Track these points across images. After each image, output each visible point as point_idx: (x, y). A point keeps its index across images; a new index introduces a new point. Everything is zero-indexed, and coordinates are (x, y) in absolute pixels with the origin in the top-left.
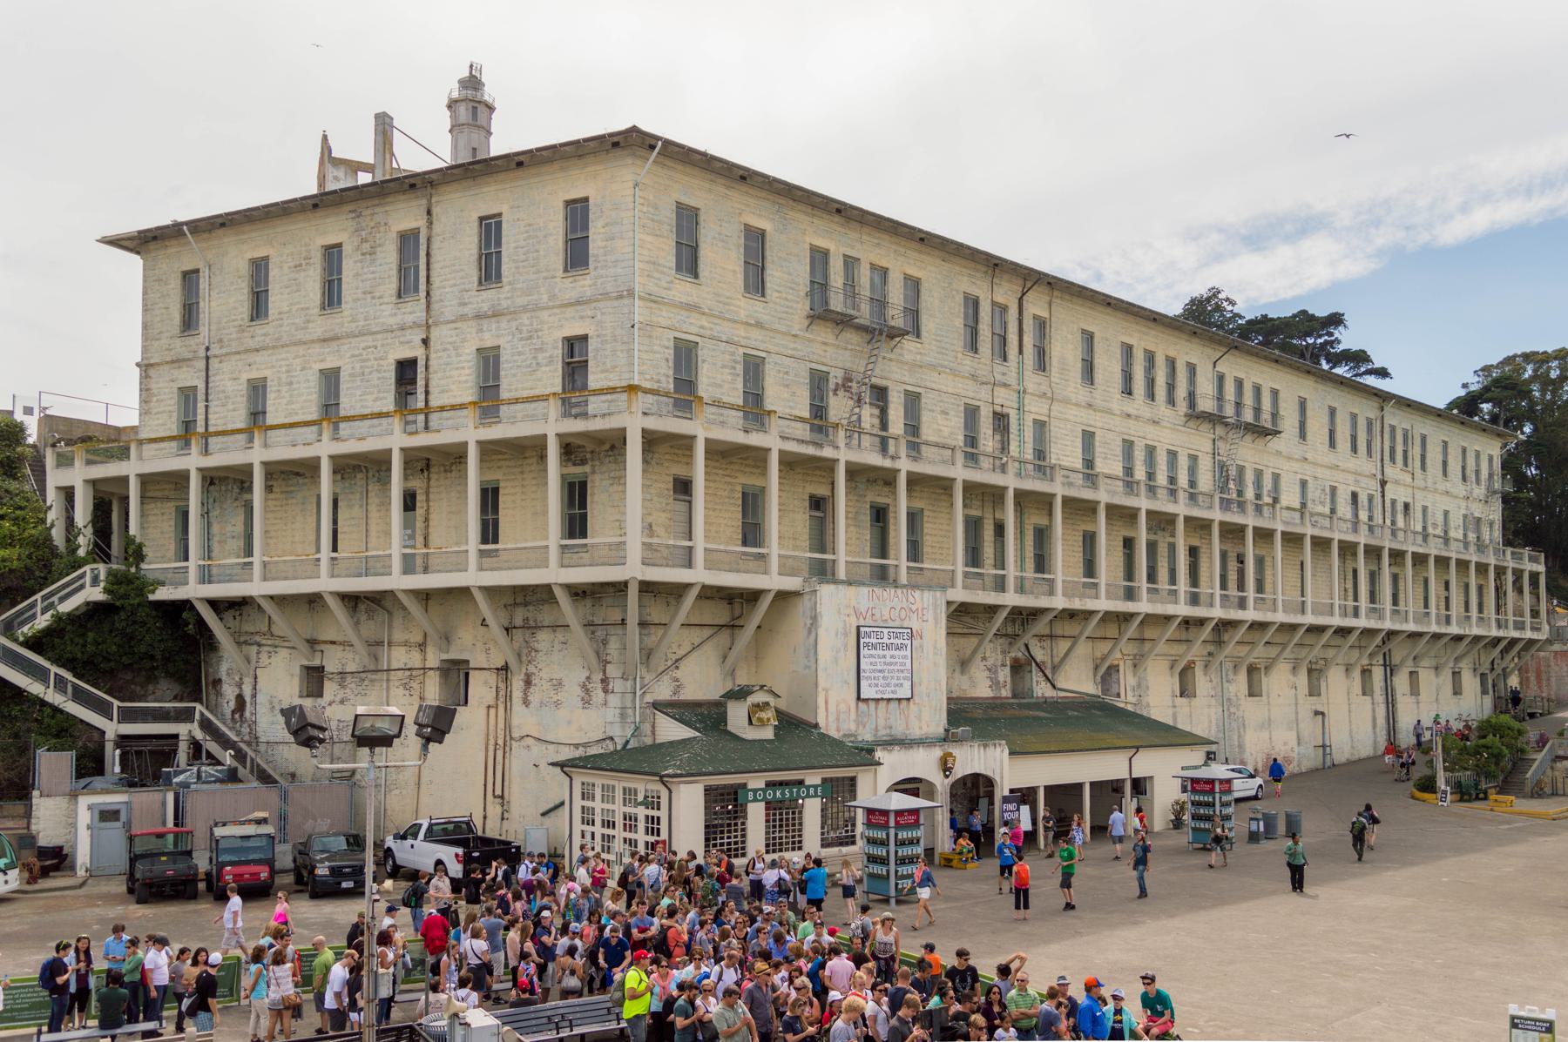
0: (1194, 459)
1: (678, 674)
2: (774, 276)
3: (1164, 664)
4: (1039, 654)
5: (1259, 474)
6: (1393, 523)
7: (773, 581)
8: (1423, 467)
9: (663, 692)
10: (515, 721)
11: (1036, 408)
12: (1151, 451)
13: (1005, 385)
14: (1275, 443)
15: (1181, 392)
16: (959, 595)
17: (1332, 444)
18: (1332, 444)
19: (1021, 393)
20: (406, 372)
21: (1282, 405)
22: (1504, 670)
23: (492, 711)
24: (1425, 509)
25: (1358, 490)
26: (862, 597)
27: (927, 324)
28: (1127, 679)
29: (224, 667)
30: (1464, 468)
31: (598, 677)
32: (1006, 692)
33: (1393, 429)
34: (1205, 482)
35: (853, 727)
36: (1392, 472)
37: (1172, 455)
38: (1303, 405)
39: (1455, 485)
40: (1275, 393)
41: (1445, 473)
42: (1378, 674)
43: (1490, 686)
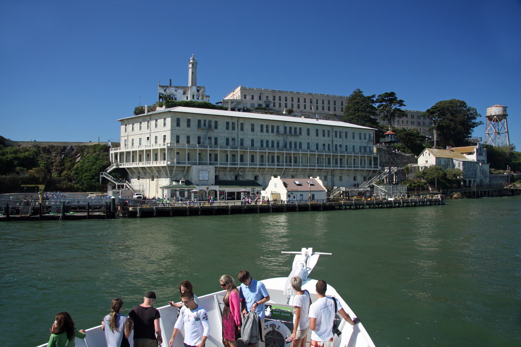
2: (192, 124)
4: (240, 173)
6: (336, 149)
7: (187, 165)
12: (267, 142)
16: (219, 166)
17: (317, 135)
18: (317, 135)
19: (238, 135)
20: (148, 138)
24: (346, 146)
26: (200, 167)
27: (219, 127)
34: (281, 145)
35: (198, 183)
36: (335, 139)
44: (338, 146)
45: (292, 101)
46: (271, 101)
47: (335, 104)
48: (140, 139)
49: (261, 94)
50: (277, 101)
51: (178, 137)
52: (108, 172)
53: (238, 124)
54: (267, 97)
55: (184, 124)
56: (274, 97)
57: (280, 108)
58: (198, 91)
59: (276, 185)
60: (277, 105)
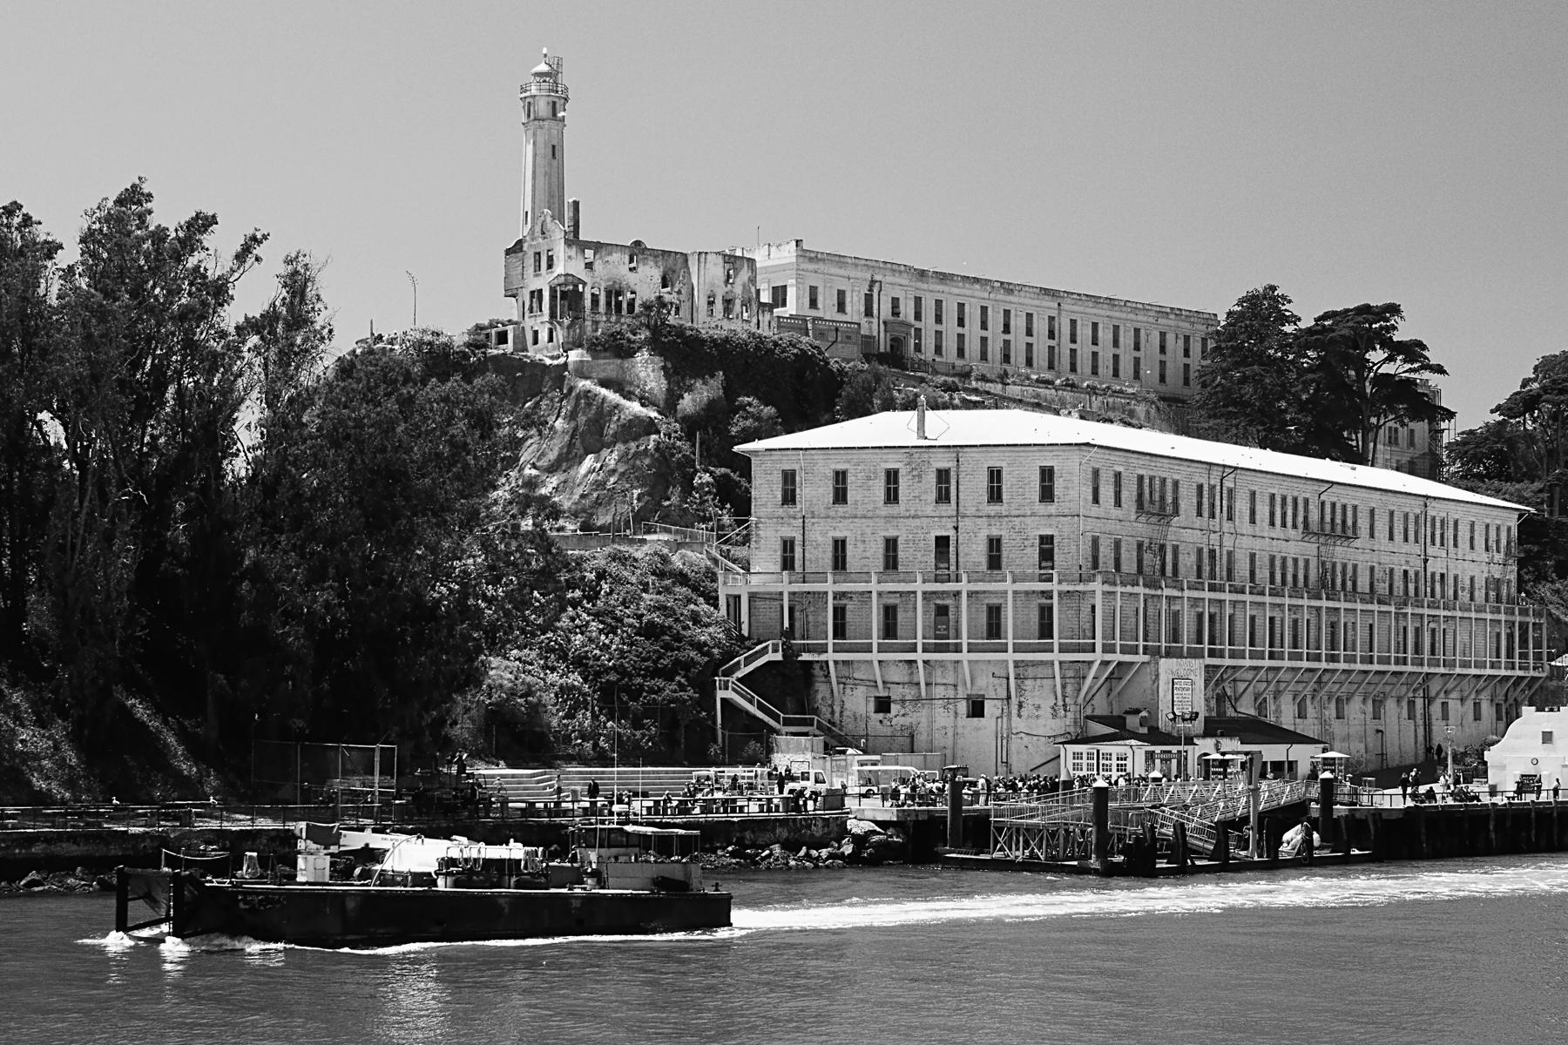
0: (1307, 562)
1: (1093, 702)
3: (1291, 697)
5: (1344, 566)
8: (1456, 545)
9: (1089, 712)
10: (1013, 725)
11: (1228, 543)
12: (1284, 560)
13: (1215, 532)
14: (1357, 543)
15: (1300, 519)
17: (1391, 538)
18: (1391, 538)
20: (942, 543)
21: (1359, 515)
22: (1515, 700)
23: (999, 720)
24: (1456, 578)
25: (1408, 568)
27: (1183, 505)
28: (1271, 706)
29: (819, 696)
30: (1487, 540)
31: (1060, 703)
32: (1214, 714)
33: (1434, 519)
36: (1430, 550)
37: (1295, 561)
39: (1480, 554)
40: (1355, 508)
41: (1472, 547)
43: (1504, 714)
44: (1438, 577)
45: (984, 326)
47: (1137, 347)
48: (891, 545)
49: (873, 282)
50: (928, 324)
51: (1095, 542)
52: (739, 674)
53: (1221, 493)
54: (895, 302)
55: (1107, 492)
56: (918, 300)
57: (937, 359)
59: (1547, 737)
60: (929, 343)
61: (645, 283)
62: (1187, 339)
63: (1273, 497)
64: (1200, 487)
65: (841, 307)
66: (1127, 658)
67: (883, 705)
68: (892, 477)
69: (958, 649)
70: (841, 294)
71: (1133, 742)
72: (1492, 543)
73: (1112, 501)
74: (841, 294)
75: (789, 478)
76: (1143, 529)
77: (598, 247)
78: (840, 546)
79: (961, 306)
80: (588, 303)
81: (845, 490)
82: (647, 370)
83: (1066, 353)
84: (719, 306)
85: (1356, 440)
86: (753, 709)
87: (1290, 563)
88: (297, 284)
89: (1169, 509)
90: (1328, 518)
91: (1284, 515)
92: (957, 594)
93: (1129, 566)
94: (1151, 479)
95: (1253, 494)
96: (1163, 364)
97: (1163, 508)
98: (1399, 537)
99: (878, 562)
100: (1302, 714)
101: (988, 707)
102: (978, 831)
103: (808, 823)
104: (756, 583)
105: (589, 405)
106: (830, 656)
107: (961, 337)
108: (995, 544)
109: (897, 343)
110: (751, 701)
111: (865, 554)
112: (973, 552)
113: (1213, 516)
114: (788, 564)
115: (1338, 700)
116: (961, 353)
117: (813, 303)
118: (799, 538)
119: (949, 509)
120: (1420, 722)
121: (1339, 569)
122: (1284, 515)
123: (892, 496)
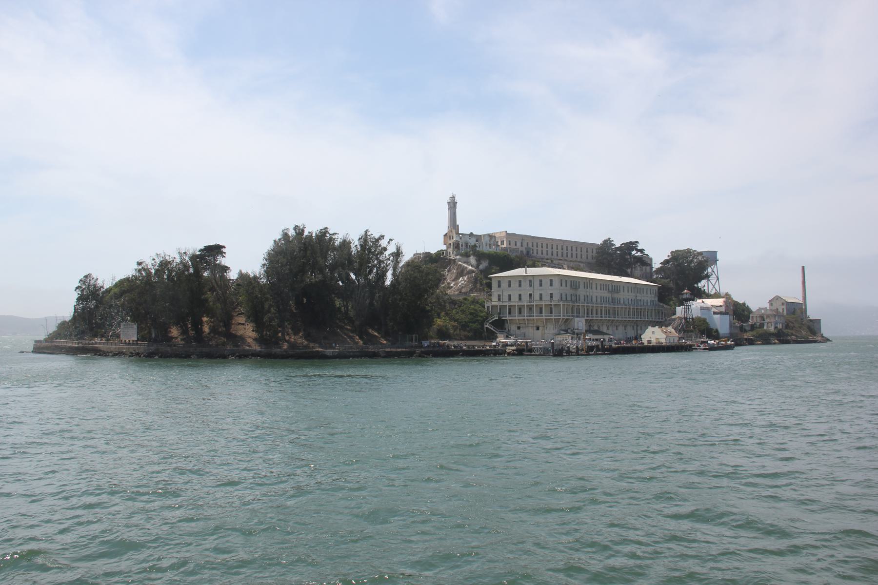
5: (617, 298)
7: (571, 318)
14: (620, 293)
16: (586, 318)
17: (628, 292)
18: (628, 292)
20: (530, 295)
24: (643, 300)
26: (578, 319)
27: (581, 286)
28: (601, 328)
36: (637, 295)
37: (606, 297)
38: (624, 287)
39: (649, 295)
42: (635, 327)
46: (530, 248)
47: (581, 251)
48: (520, 295)
49: (522, 240)
50: (535, 248)
51: (561, 294)
54: (528, 243)
55: (564, 284)
56: (532, 243)
58: (490, 241)
60: (535, 252)
61: (472, 242)
62: (592, 249)
63: (601, 284)
64: (584, 283)
65: (516, 245)
66: (568, 318)
67: (519, 328)
68: (520, 282)
69: (534, 316)
70: (516, 242)
71: (569, 335)
72: (652, 293)
73: (565, 285)
74: (516, 242)
75: (499, 282)
76: (572, 292)
77: (462, 234)
78: (510, 296)
79: (542, 244)
80: (460, 246)
81: (510, 285)
82: (472, 260)
83: (565, 253)
84: (488, 246)
85: (629, 271)
86: (492, 329)
87: (605, 298)
88: (398, 249)
89: (578, 287)
90: (613, 288)
91: (603, 288)
92: (533, 305)
93: (569, 299)
94: (574, 281)
95: (596, 284)
96: (587, 255)
97: (576, 287)
98: (630, 291)
99: (518, 300)
100: (608, 329)
101: (540, 328)
102: (530, 350)
103: (498, 350)
104: (493, 303)
105: (461, 267)
106: (508, 318)
107: (542, 250)
108: (541, 295)
109: (528, 253)
110: (492, 327)
111: (515, 298)
112: (536, 297)
113: (587, 288)
114: (499, 300)
115: (617, 326)
116: (542, 254)
117: (510, 244)
118: (501, 294)
119: (532, 288)
120: (635, 330)
121: (616, 299)
122: (603, 288)
123: (520, 285)
